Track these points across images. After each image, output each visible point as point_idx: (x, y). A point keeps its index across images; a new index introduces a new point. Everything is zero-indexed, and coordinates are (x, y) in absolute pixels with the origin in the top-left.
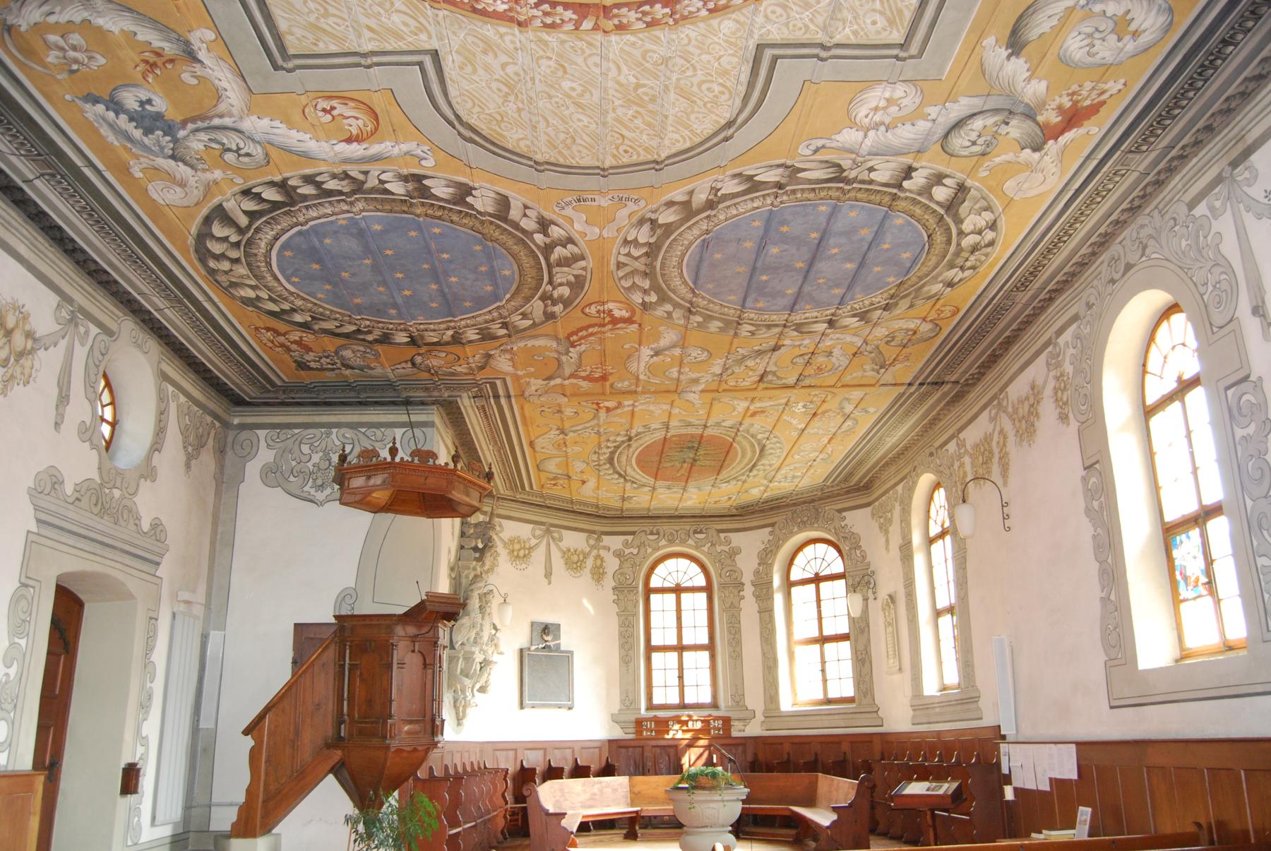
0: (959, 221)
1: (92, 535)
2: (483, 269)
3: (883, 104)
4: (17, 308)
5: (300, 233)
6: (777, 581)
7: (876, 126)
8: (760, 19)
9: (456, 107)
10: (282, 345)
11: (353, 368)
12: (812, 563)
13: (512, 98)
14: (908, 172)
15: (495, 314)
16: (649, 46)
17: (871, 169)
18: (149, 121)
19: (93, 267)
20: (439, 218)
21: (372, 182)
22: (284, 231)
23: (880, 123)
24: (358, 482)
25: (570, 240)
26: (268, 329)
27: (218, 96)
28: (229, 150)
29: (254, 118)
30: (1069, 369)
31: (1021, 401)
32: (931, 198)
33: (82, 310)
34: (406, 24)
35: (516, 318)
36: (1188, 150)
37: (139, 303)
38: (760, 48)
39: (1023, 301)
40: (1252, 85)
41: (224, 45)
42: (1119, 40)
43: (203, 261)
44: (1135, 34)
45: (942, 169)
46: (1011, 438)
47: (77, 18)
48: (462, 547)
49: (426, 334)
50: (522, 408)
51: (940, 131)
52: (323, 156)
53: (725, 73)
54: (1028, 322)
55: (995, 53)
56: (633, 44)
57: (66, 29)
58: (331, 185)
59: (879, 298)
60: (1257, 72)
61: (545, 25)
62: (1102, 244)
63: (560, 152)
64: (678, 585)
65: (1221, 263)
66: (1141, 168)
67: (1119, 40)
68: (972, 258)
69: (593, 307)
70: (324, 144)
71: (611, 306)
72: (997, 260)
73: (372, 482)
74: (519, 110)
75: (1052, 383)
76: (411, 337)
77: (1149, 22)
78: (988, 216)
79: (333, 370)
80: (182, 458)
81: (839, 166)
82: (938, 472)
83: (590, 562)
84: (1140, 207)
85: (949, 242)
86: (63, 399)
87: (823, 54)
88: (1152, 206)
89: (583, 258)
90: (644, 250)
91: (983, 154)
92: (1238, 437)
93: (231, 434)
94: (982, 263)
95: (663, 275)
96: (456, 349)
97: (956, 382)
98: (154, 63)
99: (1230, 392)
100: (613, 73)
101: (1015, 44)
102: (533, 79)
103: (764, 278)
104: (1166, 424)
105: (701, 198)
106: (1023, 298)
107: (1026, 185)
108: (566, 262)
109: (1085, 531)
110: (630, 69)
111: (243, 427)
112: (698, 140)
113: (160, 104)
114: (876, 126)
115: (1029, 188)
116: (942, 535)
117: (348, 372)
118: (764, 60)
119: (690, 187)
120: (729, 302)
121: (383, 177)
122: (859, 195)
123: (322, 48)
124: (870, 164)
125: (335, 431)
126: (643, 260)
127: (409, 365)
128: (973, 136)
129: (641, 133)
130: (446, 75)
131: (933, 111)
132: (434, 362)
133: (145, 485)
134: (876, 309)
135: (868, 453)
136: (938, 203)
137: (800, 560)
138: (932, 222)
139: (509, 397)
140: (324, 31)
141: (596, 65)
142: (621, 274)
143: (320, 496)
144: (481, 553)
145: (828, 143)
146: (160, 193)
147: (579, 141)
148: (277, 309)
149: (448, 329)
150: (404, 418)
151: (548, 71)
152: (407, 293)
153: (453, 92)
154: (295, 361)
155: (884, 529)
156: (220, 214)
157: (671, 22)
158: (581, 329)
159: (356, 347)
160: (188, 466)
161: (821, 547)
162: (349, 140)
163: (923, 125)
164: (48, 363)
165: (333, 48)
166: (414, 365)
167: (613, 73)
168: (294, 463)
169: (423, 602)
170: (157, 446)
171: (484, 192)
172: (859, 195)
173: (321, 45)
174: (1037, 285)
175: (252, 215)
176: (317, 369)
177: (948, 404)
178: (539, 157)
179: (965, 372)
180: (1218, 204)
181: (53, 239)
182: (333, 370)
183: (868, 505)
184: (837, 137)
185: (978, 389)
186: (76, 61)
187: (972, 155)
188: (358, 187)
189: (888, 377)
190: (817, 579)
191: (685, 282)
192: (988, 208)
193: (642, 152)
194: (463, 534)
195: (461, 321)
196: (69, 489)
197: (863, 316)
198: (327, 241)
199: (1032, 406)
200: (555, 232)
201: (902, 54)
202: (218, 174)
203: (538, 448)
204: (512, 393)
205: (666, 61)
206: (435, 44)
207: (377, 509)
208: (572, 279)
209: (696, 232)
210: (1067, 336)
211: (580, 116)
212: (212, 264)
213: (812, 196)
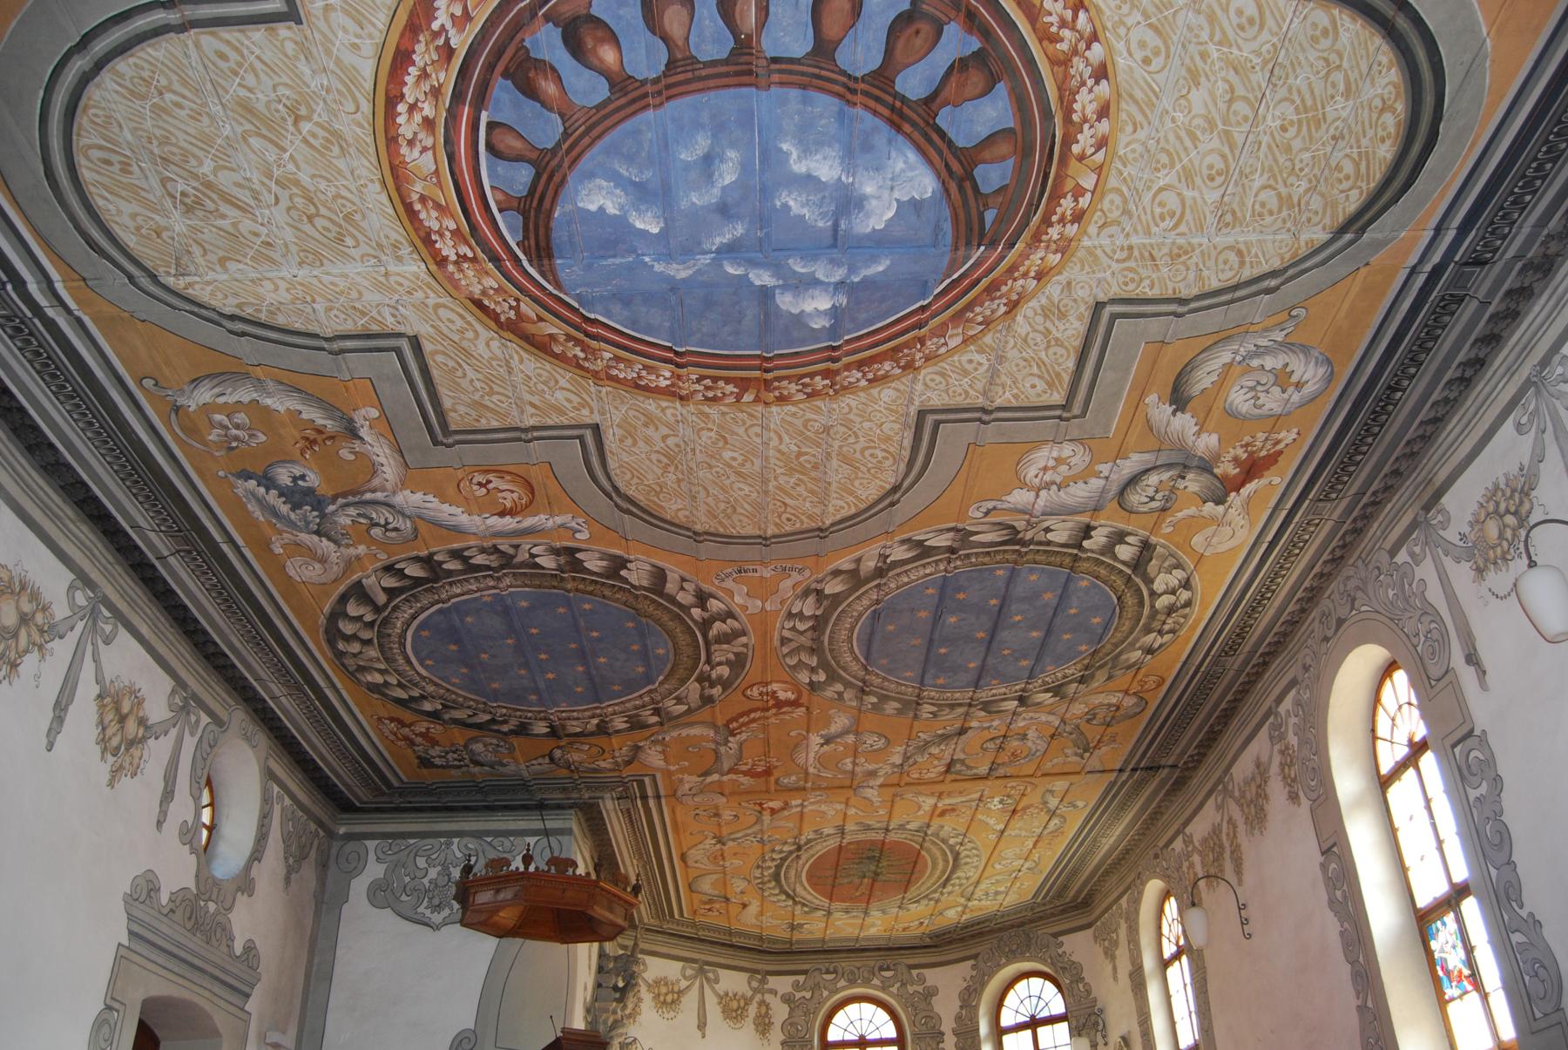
0: (1149, 581)
1: (182, 954)
2: (635, 647)
3: (1051, 463)
4: (133, 692)
5: (440, 611)
6: (984, 1028)
7: (1047, 486)
8: (919, 387)
9: (615, 478)
10: (406, 738)
11: (482, 765)
12: (1027, 1002)
13: (672, 469)
14: (1087, 531)
15: (647, 699)
16: (810, 415)
17: (1047, 530)
18: (298, 496)
19: (211, 649)
20: (591, 593)
21: (522, 556)
22: (423, 610)
23: (1052, 483)
24: (485, 897)
25: (730, 615)
26: (392, 720)
27: (374, 469)
28: (377, 525)
29: (407, 492)
30: (1293, 740)
31: (1247, 783)
32: (1115, 558)
33: (195, 697)
34: (569, 401)
35: (669, 703)
36: (1380, 497)
37: (254, 690)
38: (922, 414)
39: (1236, 667)
40: (1430, 429)
41: (388, 426)
42: (1284, 392)
43: (331, 643)
44: (1299, 386)
45: (1122, 526)
46: (1241, 827)
47: (246, 399)
48: (599, 985)
49: (569, 723)
50: (673, 811)
51: (1114, 489)
52: (474, 530)
53: (888, 439)
54: (1245, 691)
55: (1160, 411)
56: (794, 415)
57: (230, 410)
58: (480, 560)
59: (1073, 670)
60: (1432, 415)
61: (707, 399)
62: (1310, 599)
63: (720, 523)
64: (862, 1037)
65: (1429, 611)
66: (1335, 516)
67: (1284, 392)
68: (1170, 621)
70: (476, 518)
71: (775, 687)
73: (501, 896)
74: (679, 481)
75: (1277, 759)
76: (551, 727)
77: (1309, 373)
78: (1179, 574)
79: (459, 767)
80: (281, 870)
81: (1013, 527)
82: (1165, 877)
83: (752, 1010)
84: (1342, 557)
85: (1141, 603)
86: (168, 795)
87: (986, 418)
88: (1355, 556)
89: (744, 633)
90: (811, 624)
91: (1164, 510)
92: (1471, 799)
93: (336, 846)
94: (1181, 625)
95: (831, 651)
96: (602, 741)
97: (1174, 766)
98: (314, 440)
99: (1457, 750)
100: (775, 442)
101: (1179, 399)
102: (693, 450)
103: (943, 651)
104: (1403, 794)
105: (870, 564)
106: (1234, 663)
107: (1215, 540)
109: (1331, 927)
110: (792, 437)
111: (350, 837)
112: (863, 506)
113: (313, 480)
114: (1047, 486)
115: (1222, 543)
116: (1176, 956)
117: (476, 770)
118: (926, 426)
119: (858, 554)
121: (534, 551)
122: (1038, 558)
123: (483, 424)
124: (1046, 524)
125: (456, 840)
126: (809, 634)
127: (547, 760)
128: (1151, 492)
131: (1105, 468)
132: (575, 757)
133: (242, 899)
134: (1071, 682)
135: (1083, 860)
136: (1123, 563)
137: (1011, 999)
138: (1120, 583)
139: (658, 797)
140: (487, 407)
141: (757, 435)
142: (785, 650)
143: (436, 918)
144: (622, 993)
145: (999, 505)
146: (299, 570)
147: (739, 510)
148: (404, 696)
149: (593, 717)
150: (538, 825)
152: (550, 676)
153: (612, 463)
154: (419, 757)
155: (1110, 955)
156: (358, 592)
157: (831, 392)
158: (742, 715)
159: (488, 740)
160: (288, 880)
161: (1036, 982)
162: (502, 514)
163: (1096, 483)
164: (157, 752)
165: (495, 424)
166: (552, 759)
167: (775, 442)
168: (407, 879)
169: (558, 1039)
170: (257, 855)
171: (640, 565)
172: (1038, 558)
173: (483, 421)
174: (1247, 649)
175: (391, 593)
176: (442, 767)
177: (1168, 794)
178: (698, 528)
179: (1183, 753)
180: (1417, 549)
181: (175, 619)
182: (459, 767)
183: (1089, 926)
184: (1008, 498)
185: (1201, 772)
186: (237, 438)
187: (1152, 511)
188: (507, 561)
189: (1094, 762)
190: (1034, 1024)
191: (856, 658)
192: (1179, 566)
194: (600, 970)
195: (609, 707)
196: (164, 898)
197: (1057, 691)
198: (469, 619)
199: (1259, 786)
200: (714, 605)
201: (1065, 415)
202: (362, 549)
203: (691, 863)
204: (662, 793)
205: (827, 429)
206: (596, 418)
207: (501, 933)
208: (732, 657)
209: (866, 602)
210: (1287, 704)
212: (341, 646)
213: (987, 559)
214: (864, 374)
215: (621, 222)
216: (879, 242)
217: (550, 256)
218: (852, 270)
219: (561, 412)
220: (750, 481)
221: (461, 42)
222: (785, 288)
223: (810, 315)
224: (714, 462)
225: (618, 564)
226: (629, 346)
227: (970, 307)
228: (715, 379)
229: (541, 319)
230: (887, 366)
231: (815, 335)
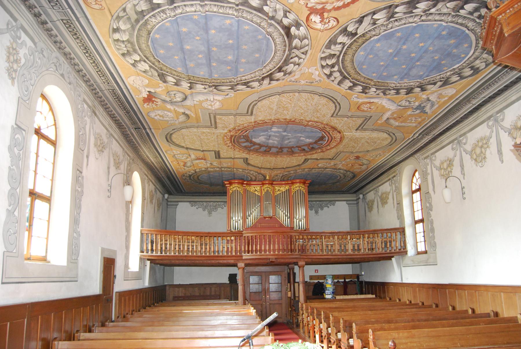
25: (323, 67)
63: (311, 96)
69: (330, 26)
71: (319, 26)
72: (110, 47)
90: (292, 60)
95: (285, 46)
103: (231, 42)
108: (332, 56)
112: (267, 99)
119: (270, 86)
120: (249, 24)
191: (274, 40)
200: (327, 71)
208: (333, 47)
209: (268, 68)
213: (223, 81)
216: (263, 135)
222: (281, 132)
226: (315, 127)
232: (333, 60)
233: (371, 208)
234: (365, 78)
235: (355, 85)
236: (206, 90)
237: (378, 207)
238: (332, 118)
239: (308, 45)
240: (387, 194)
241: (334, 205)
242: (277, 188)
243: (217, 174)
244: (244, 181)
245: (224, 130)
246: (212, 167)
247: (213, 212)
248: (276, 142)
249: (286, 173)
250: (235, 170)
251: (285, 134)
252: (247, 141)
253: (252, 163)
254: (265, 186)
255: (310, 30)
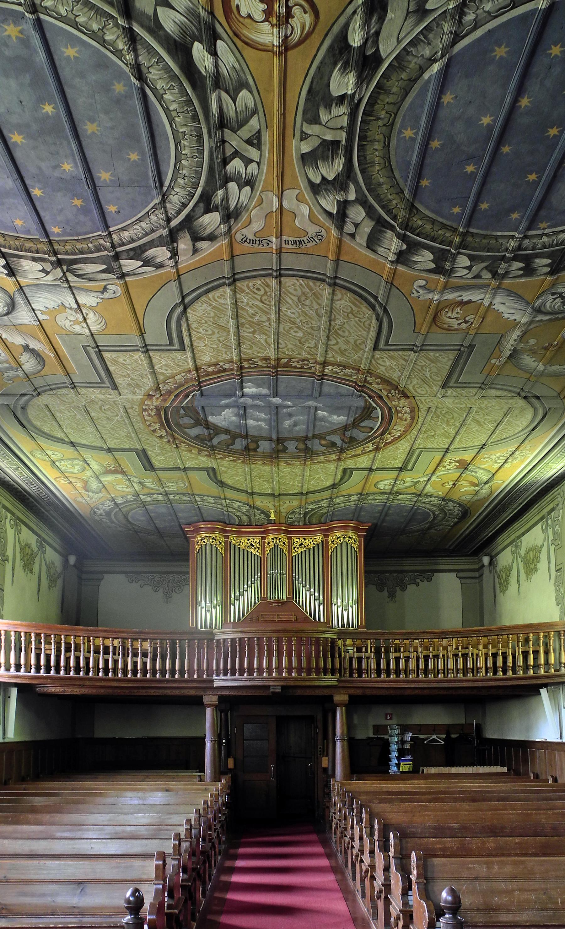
16: (250, 351)
25: (315, 189)
34: (384, 361)
56: (258, 352)
63: (311, 289)
108: (328, 149)
110: (260, 342)
112: (204, 298)
119: (197, 258)
129: (248, 304)
130: (373, 343)
147: (296, 299)
151: (310, 341)
191: (160, 98)
193: (245, 288)
200: (330, 203)
211: (293, 315)
214: (222, 367)
215: (331, 413)
216: (227, 406)
217: (365, 408)
218: (236, 402)
219: (391, 357)
220: (286, 318)
221: (370, 445)
222: (266, 396)
223: (253, 387)
224: (309, 330)
225: (402, 258)
227: (177, 388)
228: (301, 368)
229: (381, 390)
230: (210, 369)
231: (250, 381)
232: (336, 162)
233: (505, 585)
234: (433, 222)
235: (414, 247)
236: (50, 278)
237: (518, 581)
238: (378, 354)
239: (255, 112)
240: (537, 550)
241: (429, 579)
242: (296, 540)
243: (163, 510)
244: (225, 524)
245: (134, 393)
246: (146, 491)
247: (174, 594)
248: (263, 424)
249: (311, 506)
250: (198, 498)
251: (277, 400)
252: (198, 423)
253: (230, 482)
254: (271, 536)
255: (248, 52)
